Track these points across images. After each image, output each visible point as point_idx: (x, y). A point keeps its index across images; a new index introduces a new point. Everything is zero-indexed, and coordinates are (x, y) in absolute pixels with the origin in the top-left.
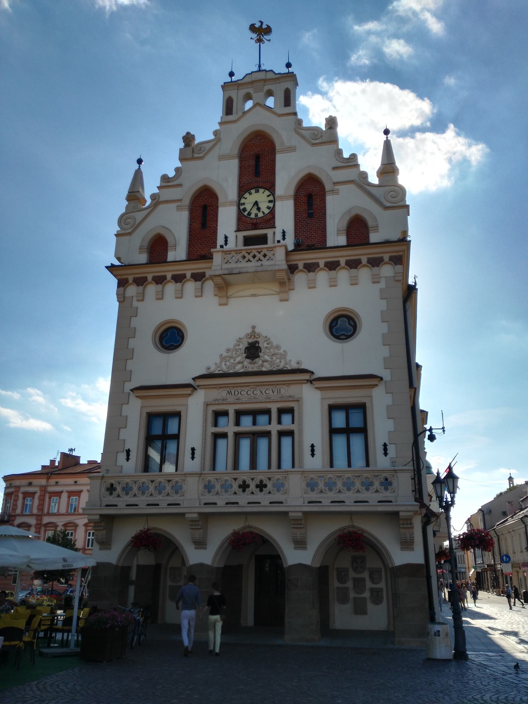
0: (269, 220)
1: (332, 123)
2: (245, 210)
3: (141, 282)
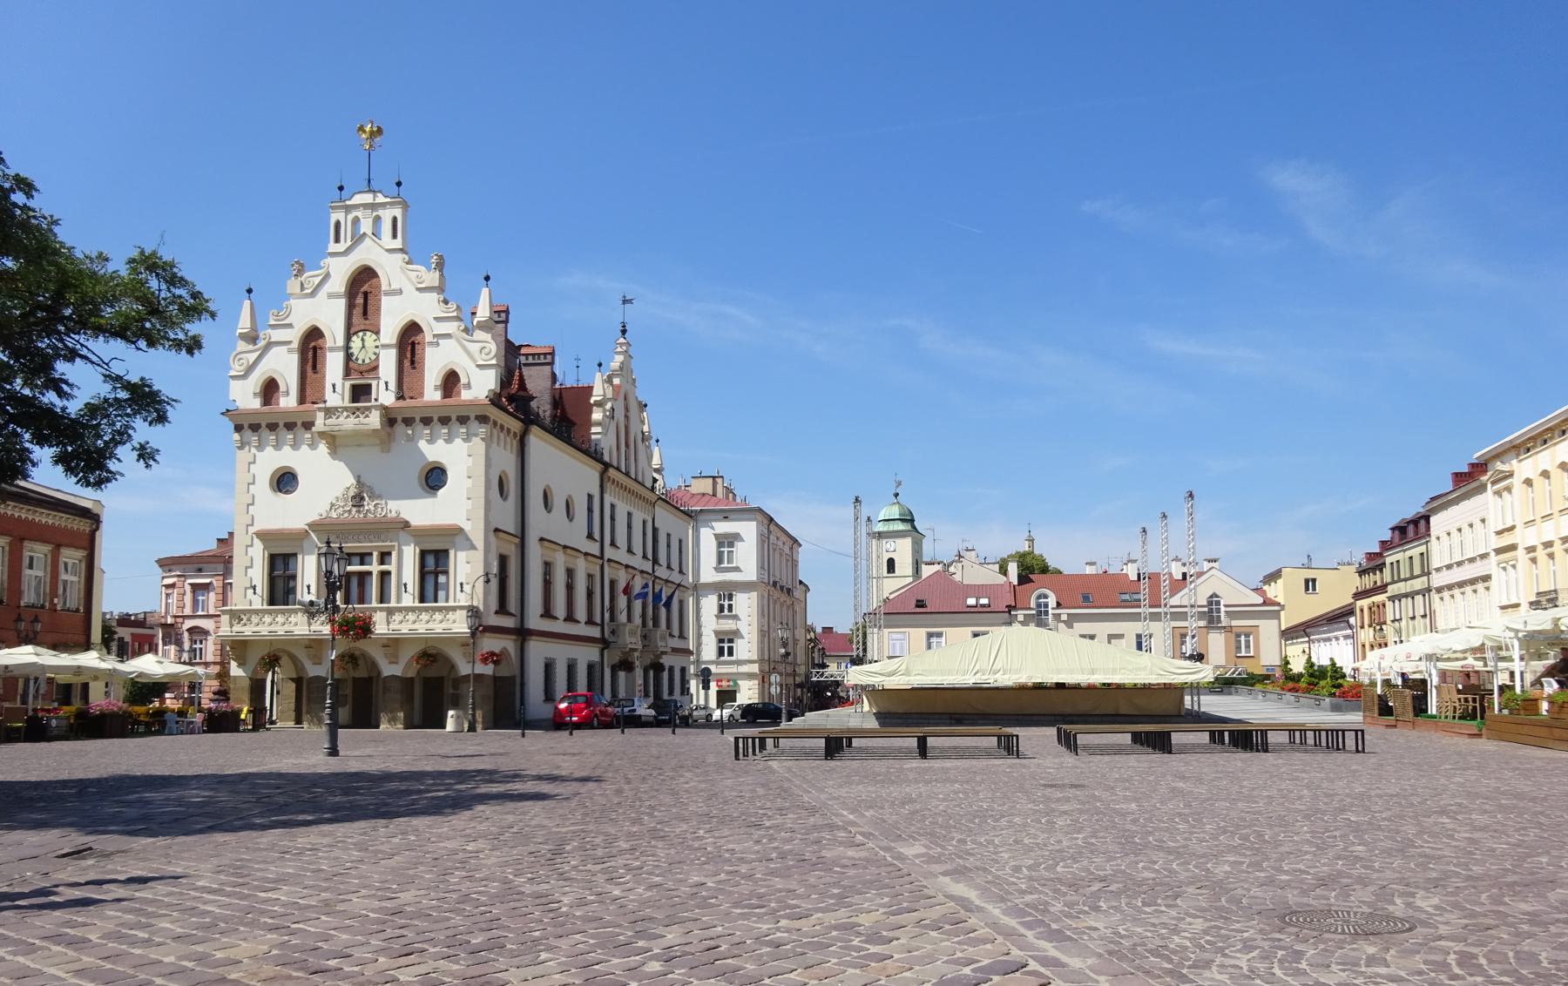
3: (255, 428)
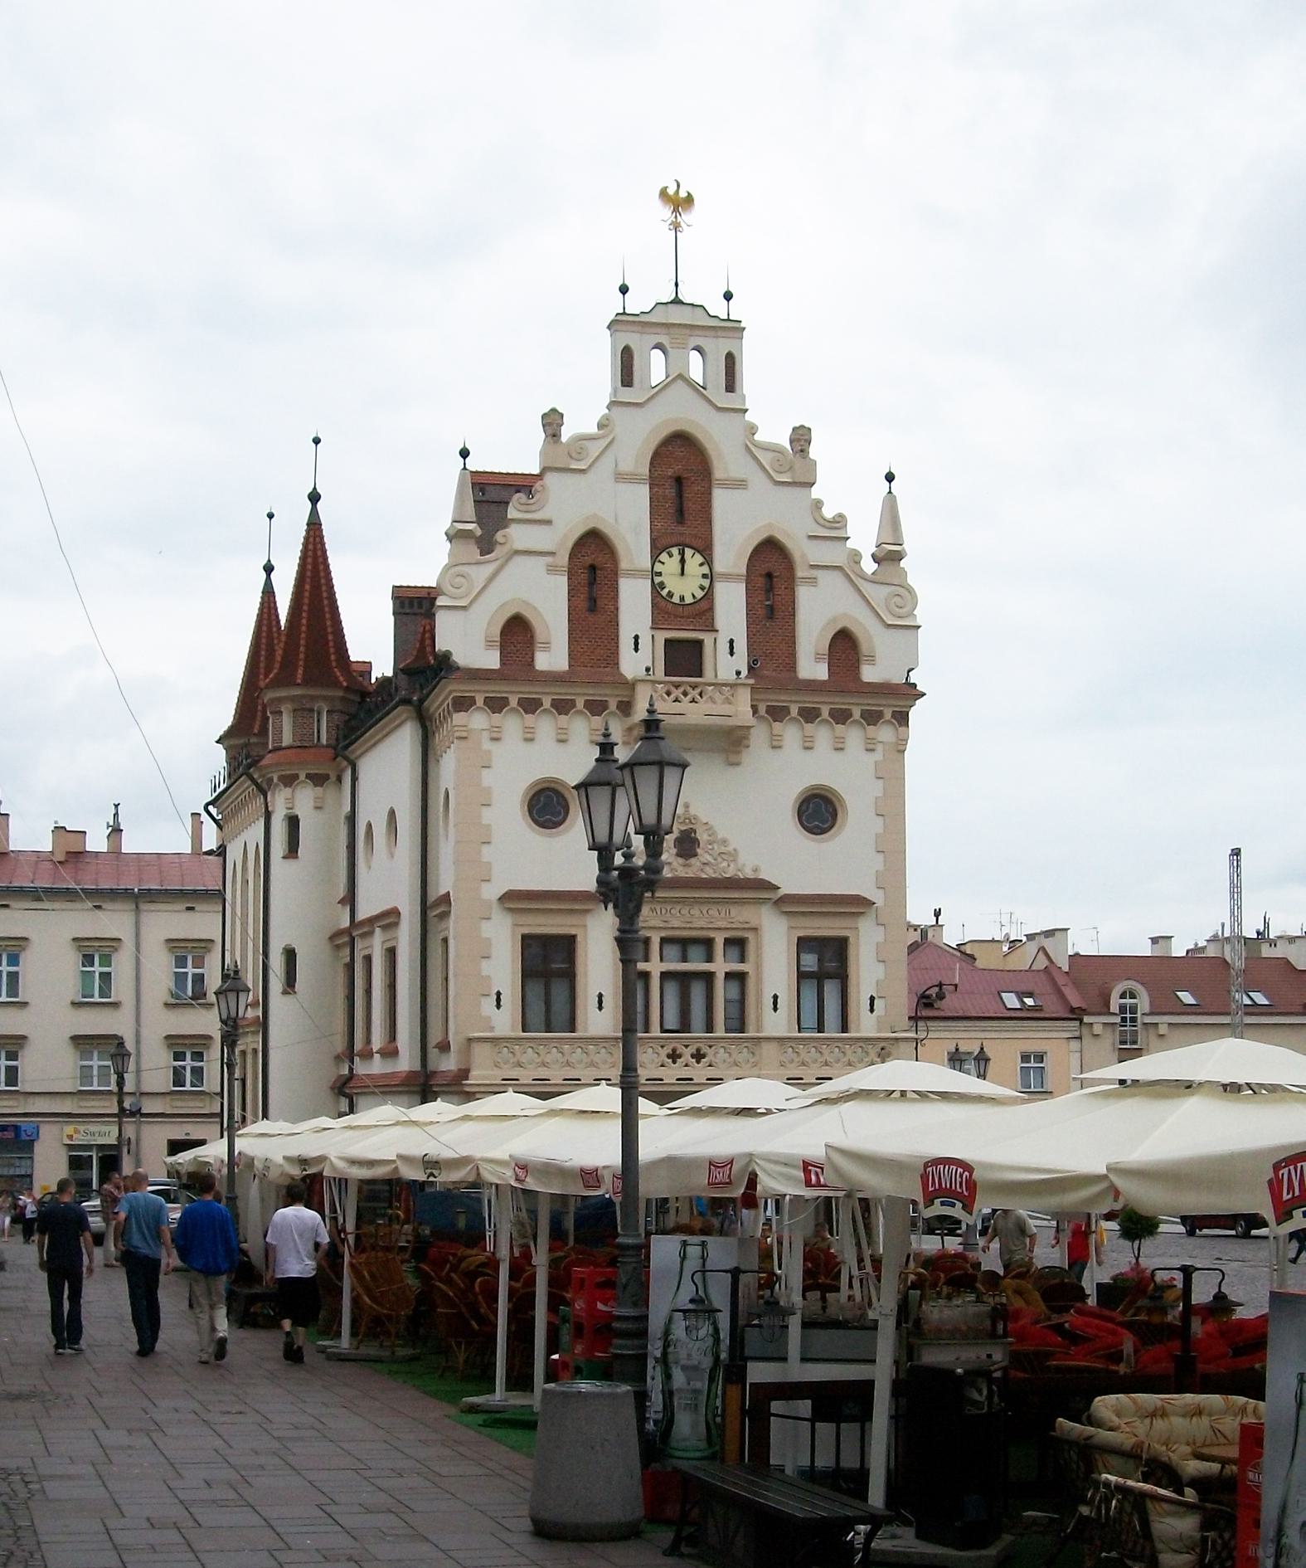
0: (702, 611)
1: (801, 437)
2: (662, 585)
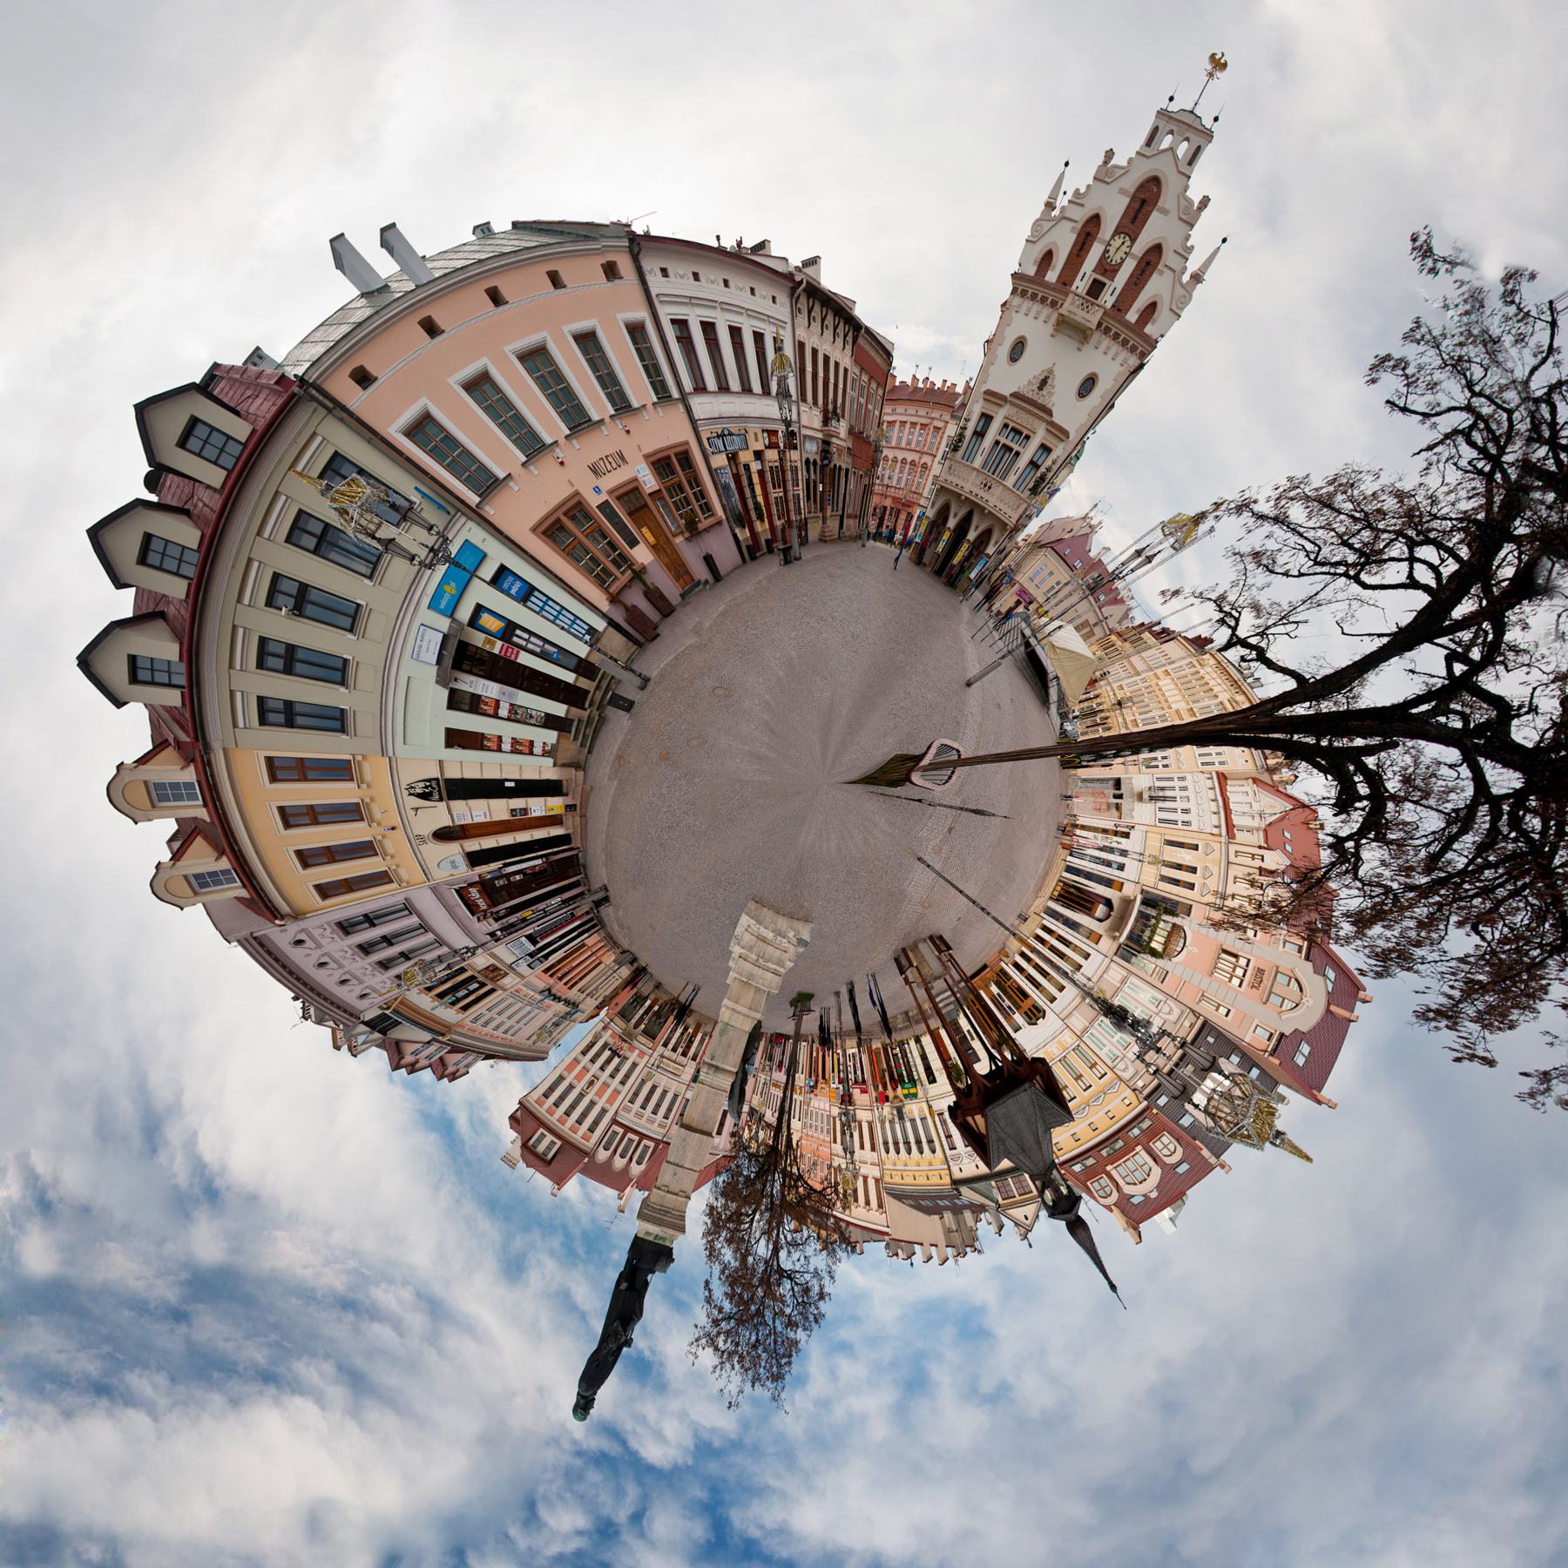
1: (1205, 201)
